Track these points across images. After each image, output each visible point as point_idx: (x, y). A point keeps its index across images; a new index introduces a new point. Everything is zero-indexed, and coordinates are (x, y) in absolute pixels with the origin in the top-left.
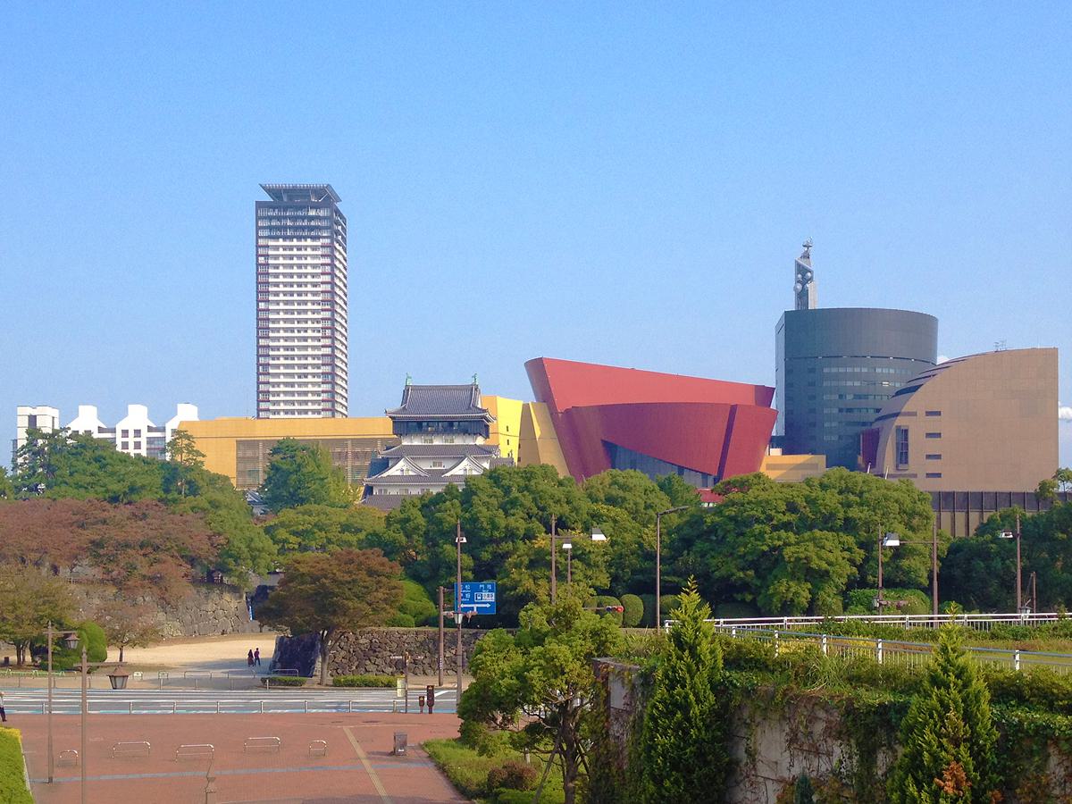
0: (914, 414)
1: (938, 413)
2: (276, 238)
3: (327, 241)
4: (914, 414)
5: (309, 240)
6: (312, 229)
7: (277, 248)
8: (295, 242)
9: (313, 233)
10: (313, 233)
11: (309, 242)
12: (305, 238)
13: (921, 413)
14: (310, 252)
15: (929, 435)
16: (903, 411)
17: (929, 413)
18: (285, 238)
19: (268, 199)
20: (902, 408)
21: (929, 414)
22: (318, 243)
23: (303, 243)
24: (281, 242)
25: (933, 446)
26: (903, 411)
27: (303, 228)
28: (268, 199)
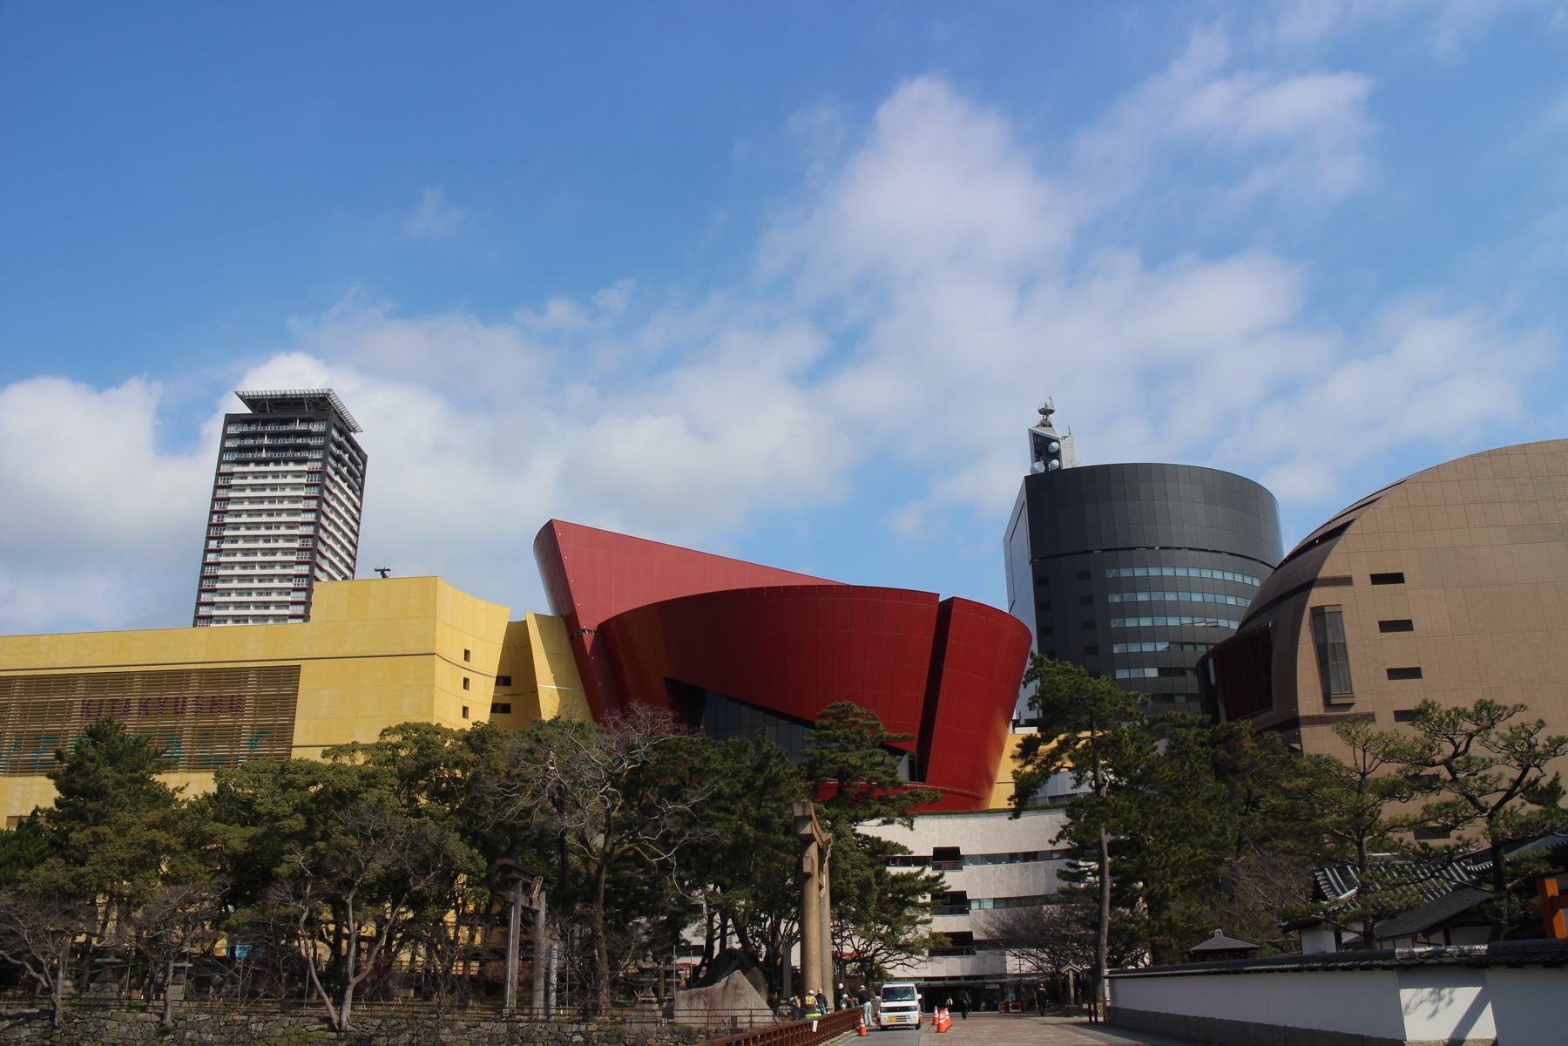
0: (1346, 581)
1: (1397, 578)
2: (246, 463)
3: (318, 465)
4: (1346, 581)
7: (244, 475)
8: (272, 467)
11: (292, 467)
12: (286, 462)
14: (290, 478)
15: (1386, 626)
16: (1323, 574)
17: (1377, 579)
18: (258, 462)
19: (246, 410)
20: (1319, 567)
21: (1377, 579)
22: (305, 467)
23: (282, 468)
24: (252, 468)
25: (1398, 650)
26: (1323, 574)
27: (285, 448)
28: (246, 410)
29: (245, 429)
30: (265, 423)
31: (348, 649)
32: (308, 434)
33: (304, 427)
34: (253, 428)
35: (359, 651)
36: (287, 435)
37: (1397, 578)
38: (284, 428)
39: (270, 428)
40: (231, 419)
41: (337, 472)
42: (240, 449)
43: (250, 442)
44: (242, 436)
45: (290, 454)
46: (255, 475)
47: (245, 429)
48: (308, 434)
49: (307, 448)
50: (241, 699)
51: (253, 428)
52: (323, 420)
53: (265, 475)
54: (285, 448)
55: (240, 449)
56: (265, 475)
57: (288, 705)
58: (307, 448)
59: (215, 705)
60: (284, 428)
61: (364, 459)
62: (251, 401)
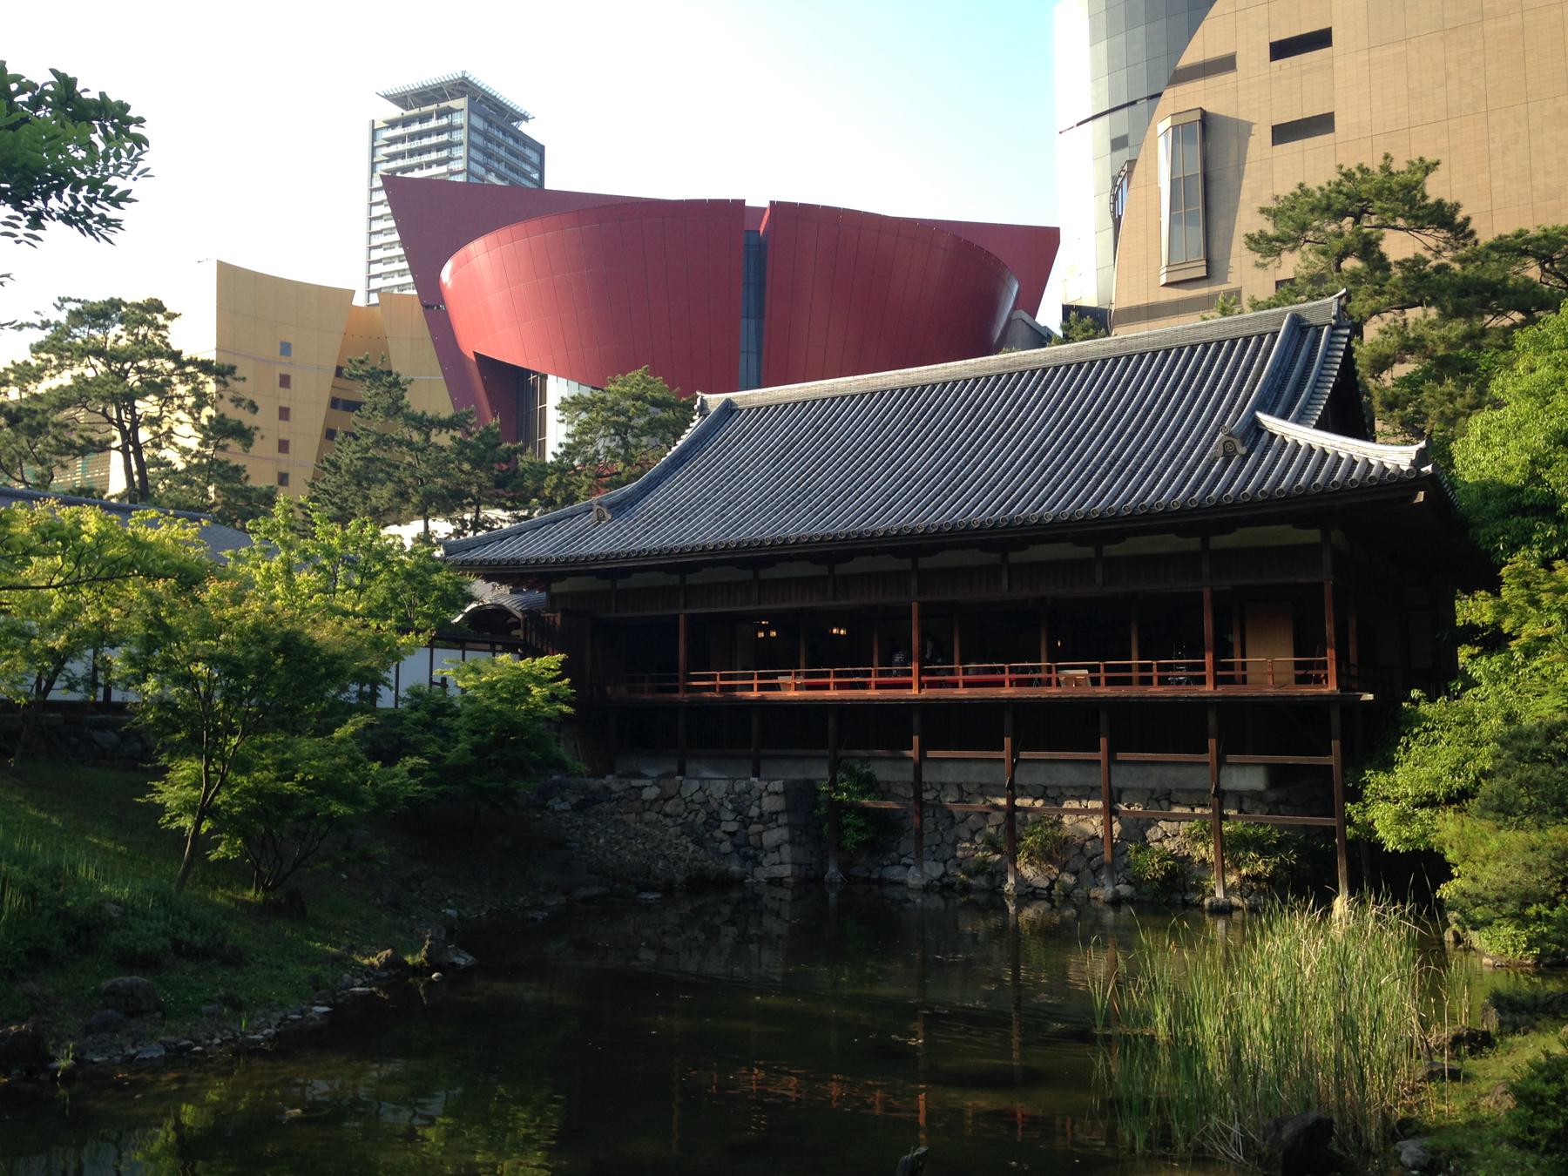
0: (1226, 64)
1: (1321, 39)
4: (1226, 64)
5: (434, 166)
13: (1253, 57)
17: (1281, 50)
19: (396, 112)
21: (1281, 50)
28: (396, 112)
30: (406, 122)
33: (444, 121)
36: (428, 133)
37: (1321, 39)
38: (425, 126)
49: (449, 145)
60: (425, 126)
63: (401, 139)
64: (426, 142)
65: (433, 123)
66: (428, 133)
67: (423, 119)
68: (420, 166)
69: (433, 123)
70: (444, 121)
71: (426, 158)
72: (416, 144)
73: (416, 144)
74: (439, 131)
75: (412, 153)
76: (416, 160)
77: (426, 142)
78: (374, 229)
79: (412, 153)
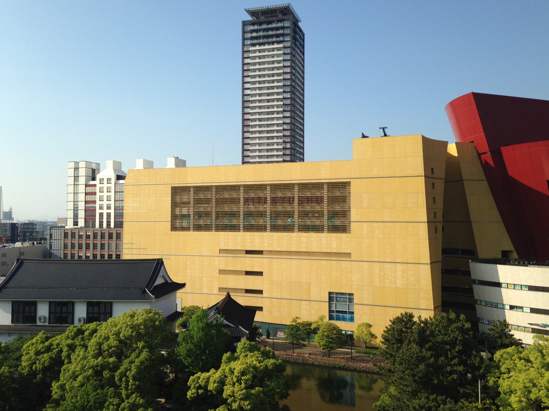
3: (288, 44)
5: (276, 44)
6: (278, 36)
7: (254, 51)
8: (267, 47)
9: (278, 39)
10: (278, 39)
11: (276, 46)
18: (260, 44)
19: (249, 18)
24: (257, 47)
27: (272, 36)
28: (249, 18)
29: (252, 28)
30: (260, 24)
31: (375, 173)
32: (283, 28)
33: (280, 25)
34: (256, 27)
35: (381, 174)
39: (265, 26)
40: (245, 24)
41: (296, 45)
42: (252, 38)
43: (255, 34)
44: (252, 31)
45: (274, 39)
46: (260, 51)
47: (252, 28)
48: (283, 28)
49: (283, 35)
50: (322, 198)
51: (256, 27)
52: (288, 20)
53: (264, 50)
54: (272, 36)
55: (252, 38)
56: (264, 50)
57: (344, 199)
58: (283, 35)
59: (309, 200)
60: (270, 26)
61: (303, 35)
62: (252, 13)
63: (256, 31)
64: (270, 33)
65: (274, 25)
66: (272, 29)
67: (269, 23)
68: (269, 43)
69: (274, 25)
70: (280, 25)
71: (270, 40)
72: (265, 33)
73: (265, 33)
74: (277, 29)
75: (264, 37)
76: (265, 40)
77: (270, 33)
78: (245, 68)
79: (264, 37)
